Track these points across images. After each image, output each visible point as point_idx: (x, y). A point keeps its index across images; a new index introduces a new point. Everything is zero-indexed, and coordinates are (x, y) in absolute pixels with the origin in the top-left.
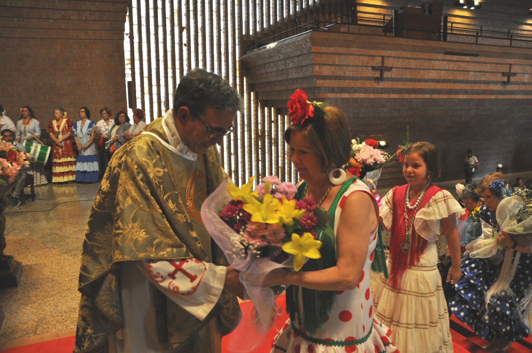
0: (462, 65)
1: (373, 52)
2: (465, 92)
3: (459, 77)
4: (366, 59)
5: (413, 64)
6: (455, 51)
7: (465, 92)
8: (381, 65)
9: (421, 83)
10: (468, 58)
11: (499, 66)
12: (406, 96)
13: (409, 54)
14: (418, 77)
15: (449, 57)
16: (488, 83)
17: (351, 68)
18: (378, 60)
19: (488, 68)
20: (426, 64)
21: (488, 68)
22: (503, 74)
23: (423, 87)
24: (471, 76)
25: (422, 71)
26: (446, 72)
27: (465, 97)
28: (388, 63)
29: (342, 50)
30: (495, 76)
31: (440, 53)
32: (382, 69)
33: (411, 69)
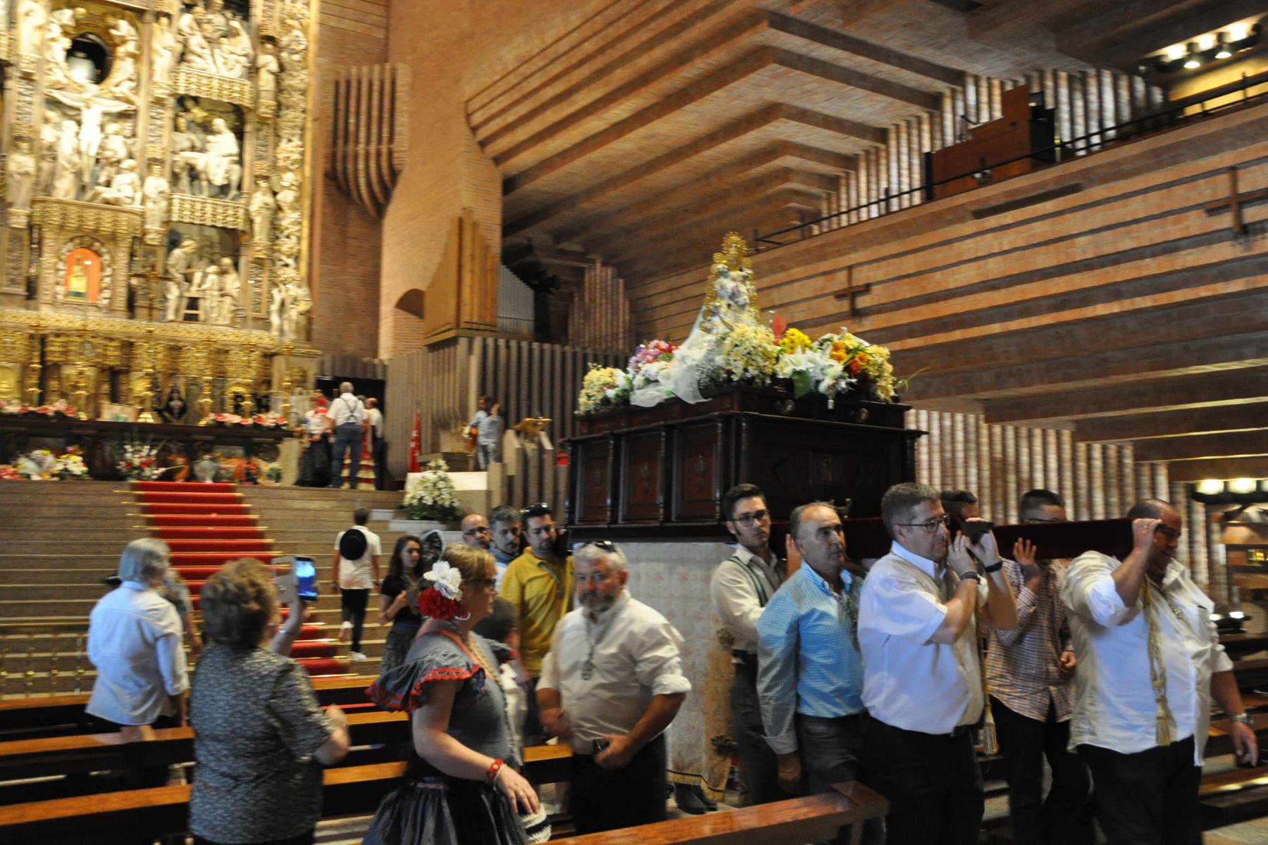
0: (1042, 230)
1: (827, 265)
2: (1114, 292)
3: (1044, 259)
4: (820, 281)
5: (910, 264)
6: (994, 203)
7: (1114, 292)
8: (845, 286)
9: (951, 302)
10: (1049, 206)
11: (1178, 190)
12: (941, 338)
13: (893, 247)
14: (930, 289)
15: (992, 221)
16: (1169, 248)
17: (803, 306)
18: (842, 276)
19: (1137, 208)
20: (941, 256)
21: (1137, 208)
22: (1213, 209)
23: (959, 309)
24: (1083, 249)
25: (938, 275)
26: (999, 258)
27: (1115, 308)
28: (860, 277)
29: (780, 277)
30: (1175, 223)
31: (961, 220)
32: (852, 293)
33: (909, 276)
